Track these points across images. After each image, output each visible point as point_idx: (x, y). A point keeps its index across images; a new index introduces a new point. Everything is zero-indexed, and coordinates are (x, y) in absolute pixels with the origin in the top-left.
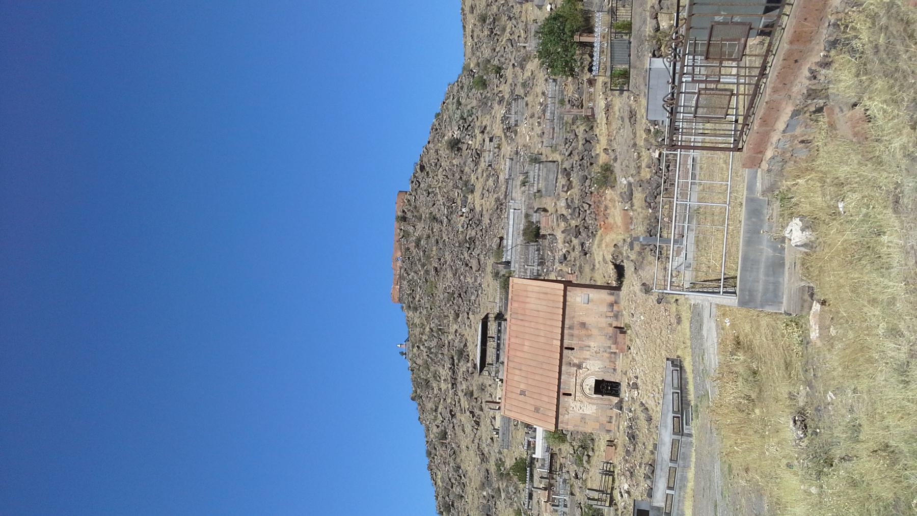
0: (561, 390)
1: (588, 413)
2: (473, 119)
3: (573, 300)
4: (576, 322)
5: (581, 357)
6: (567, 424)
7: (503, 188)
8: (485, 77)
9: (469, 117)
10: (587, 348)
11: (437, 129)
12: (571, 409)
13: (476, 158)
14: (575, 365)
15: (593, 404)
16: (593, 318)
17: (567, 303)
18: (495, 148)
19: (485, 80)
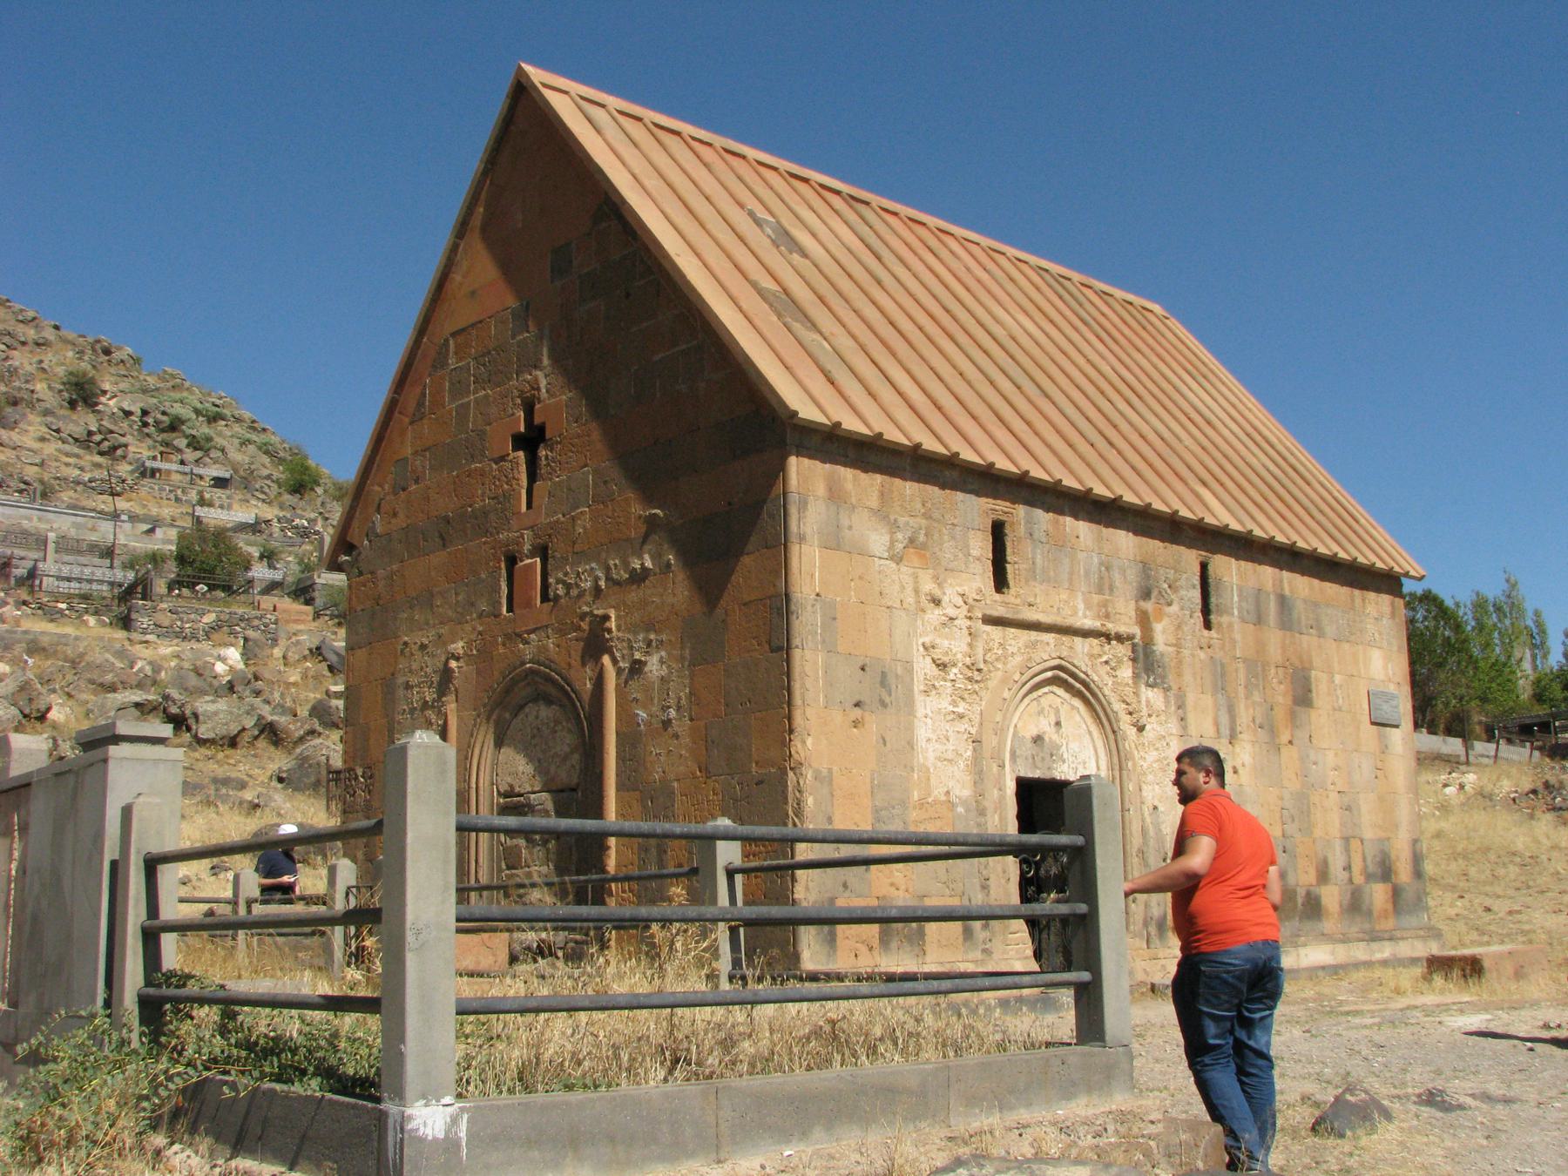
0: (1021, 511)
1: (923, 732)
2: (179, 450)
3: (1370, 627)
4: (1305, 638)
5: (1188, 677)
6: (834, 542)
7: (90, 504)
8: (320, 490)
9: (185, 442)
10: (1224, 719)
11: (107, 352)
12: (928, 586)
13: (99, 444)
14: (1144, 620)
15: (977, 771)
16: (1330, 759)
17: (1357, 592)
18: (201, 493)
19: (312, 489)
